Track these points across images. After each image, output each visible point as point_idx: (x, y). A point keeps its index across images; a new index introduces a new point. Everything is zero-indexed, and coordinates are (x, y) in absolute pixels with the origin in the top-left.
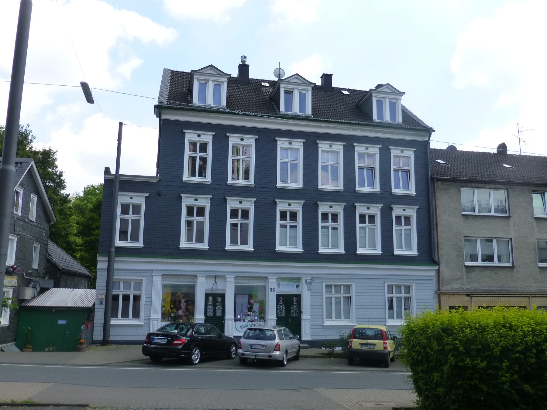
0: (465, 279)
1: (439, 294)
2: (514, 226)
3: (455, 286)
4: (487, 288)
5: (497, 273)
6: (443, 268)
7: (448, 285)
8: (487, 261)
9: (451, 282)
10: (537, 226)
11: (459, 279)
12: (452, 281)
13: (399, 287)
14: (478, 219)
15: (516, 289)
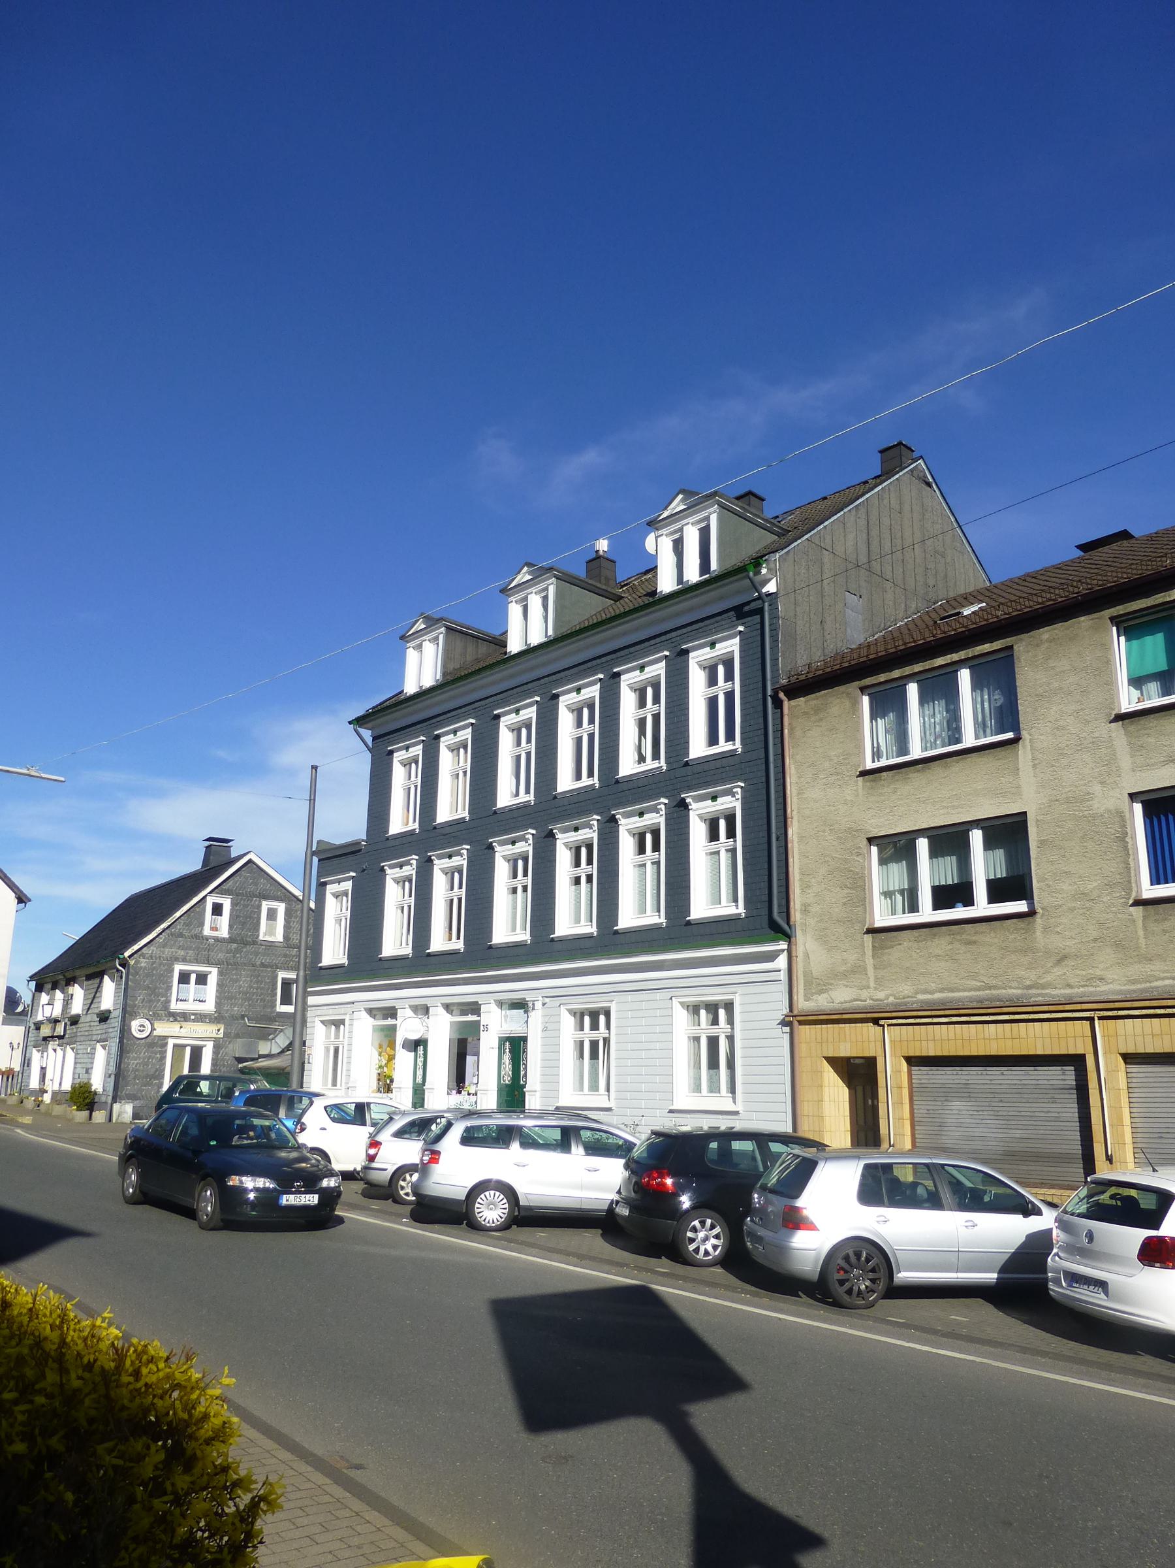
0: (871, 971)
1: (792, 1021)
2: (1034, 766)
3: (841, 997)
4: (937, 996)
5: (975, 942)
6: (805, 941)
7: (821, 992)
8: (960, 904)
9: (831, 984)
10: (1130, 744)
11: (854, 972)
12: (832, 982)
13: (712, 1008)
14: (911, 775)
15: (1043, 992)
